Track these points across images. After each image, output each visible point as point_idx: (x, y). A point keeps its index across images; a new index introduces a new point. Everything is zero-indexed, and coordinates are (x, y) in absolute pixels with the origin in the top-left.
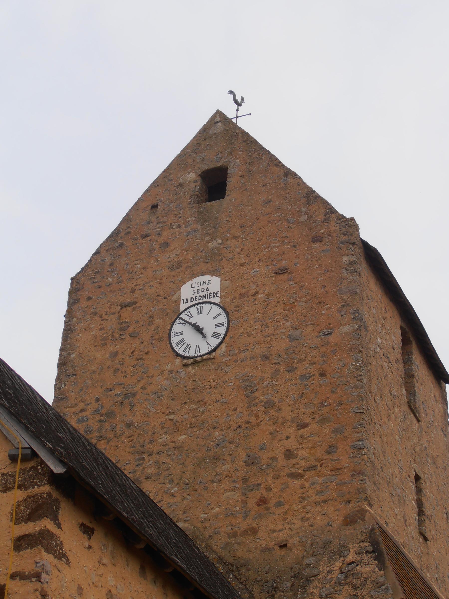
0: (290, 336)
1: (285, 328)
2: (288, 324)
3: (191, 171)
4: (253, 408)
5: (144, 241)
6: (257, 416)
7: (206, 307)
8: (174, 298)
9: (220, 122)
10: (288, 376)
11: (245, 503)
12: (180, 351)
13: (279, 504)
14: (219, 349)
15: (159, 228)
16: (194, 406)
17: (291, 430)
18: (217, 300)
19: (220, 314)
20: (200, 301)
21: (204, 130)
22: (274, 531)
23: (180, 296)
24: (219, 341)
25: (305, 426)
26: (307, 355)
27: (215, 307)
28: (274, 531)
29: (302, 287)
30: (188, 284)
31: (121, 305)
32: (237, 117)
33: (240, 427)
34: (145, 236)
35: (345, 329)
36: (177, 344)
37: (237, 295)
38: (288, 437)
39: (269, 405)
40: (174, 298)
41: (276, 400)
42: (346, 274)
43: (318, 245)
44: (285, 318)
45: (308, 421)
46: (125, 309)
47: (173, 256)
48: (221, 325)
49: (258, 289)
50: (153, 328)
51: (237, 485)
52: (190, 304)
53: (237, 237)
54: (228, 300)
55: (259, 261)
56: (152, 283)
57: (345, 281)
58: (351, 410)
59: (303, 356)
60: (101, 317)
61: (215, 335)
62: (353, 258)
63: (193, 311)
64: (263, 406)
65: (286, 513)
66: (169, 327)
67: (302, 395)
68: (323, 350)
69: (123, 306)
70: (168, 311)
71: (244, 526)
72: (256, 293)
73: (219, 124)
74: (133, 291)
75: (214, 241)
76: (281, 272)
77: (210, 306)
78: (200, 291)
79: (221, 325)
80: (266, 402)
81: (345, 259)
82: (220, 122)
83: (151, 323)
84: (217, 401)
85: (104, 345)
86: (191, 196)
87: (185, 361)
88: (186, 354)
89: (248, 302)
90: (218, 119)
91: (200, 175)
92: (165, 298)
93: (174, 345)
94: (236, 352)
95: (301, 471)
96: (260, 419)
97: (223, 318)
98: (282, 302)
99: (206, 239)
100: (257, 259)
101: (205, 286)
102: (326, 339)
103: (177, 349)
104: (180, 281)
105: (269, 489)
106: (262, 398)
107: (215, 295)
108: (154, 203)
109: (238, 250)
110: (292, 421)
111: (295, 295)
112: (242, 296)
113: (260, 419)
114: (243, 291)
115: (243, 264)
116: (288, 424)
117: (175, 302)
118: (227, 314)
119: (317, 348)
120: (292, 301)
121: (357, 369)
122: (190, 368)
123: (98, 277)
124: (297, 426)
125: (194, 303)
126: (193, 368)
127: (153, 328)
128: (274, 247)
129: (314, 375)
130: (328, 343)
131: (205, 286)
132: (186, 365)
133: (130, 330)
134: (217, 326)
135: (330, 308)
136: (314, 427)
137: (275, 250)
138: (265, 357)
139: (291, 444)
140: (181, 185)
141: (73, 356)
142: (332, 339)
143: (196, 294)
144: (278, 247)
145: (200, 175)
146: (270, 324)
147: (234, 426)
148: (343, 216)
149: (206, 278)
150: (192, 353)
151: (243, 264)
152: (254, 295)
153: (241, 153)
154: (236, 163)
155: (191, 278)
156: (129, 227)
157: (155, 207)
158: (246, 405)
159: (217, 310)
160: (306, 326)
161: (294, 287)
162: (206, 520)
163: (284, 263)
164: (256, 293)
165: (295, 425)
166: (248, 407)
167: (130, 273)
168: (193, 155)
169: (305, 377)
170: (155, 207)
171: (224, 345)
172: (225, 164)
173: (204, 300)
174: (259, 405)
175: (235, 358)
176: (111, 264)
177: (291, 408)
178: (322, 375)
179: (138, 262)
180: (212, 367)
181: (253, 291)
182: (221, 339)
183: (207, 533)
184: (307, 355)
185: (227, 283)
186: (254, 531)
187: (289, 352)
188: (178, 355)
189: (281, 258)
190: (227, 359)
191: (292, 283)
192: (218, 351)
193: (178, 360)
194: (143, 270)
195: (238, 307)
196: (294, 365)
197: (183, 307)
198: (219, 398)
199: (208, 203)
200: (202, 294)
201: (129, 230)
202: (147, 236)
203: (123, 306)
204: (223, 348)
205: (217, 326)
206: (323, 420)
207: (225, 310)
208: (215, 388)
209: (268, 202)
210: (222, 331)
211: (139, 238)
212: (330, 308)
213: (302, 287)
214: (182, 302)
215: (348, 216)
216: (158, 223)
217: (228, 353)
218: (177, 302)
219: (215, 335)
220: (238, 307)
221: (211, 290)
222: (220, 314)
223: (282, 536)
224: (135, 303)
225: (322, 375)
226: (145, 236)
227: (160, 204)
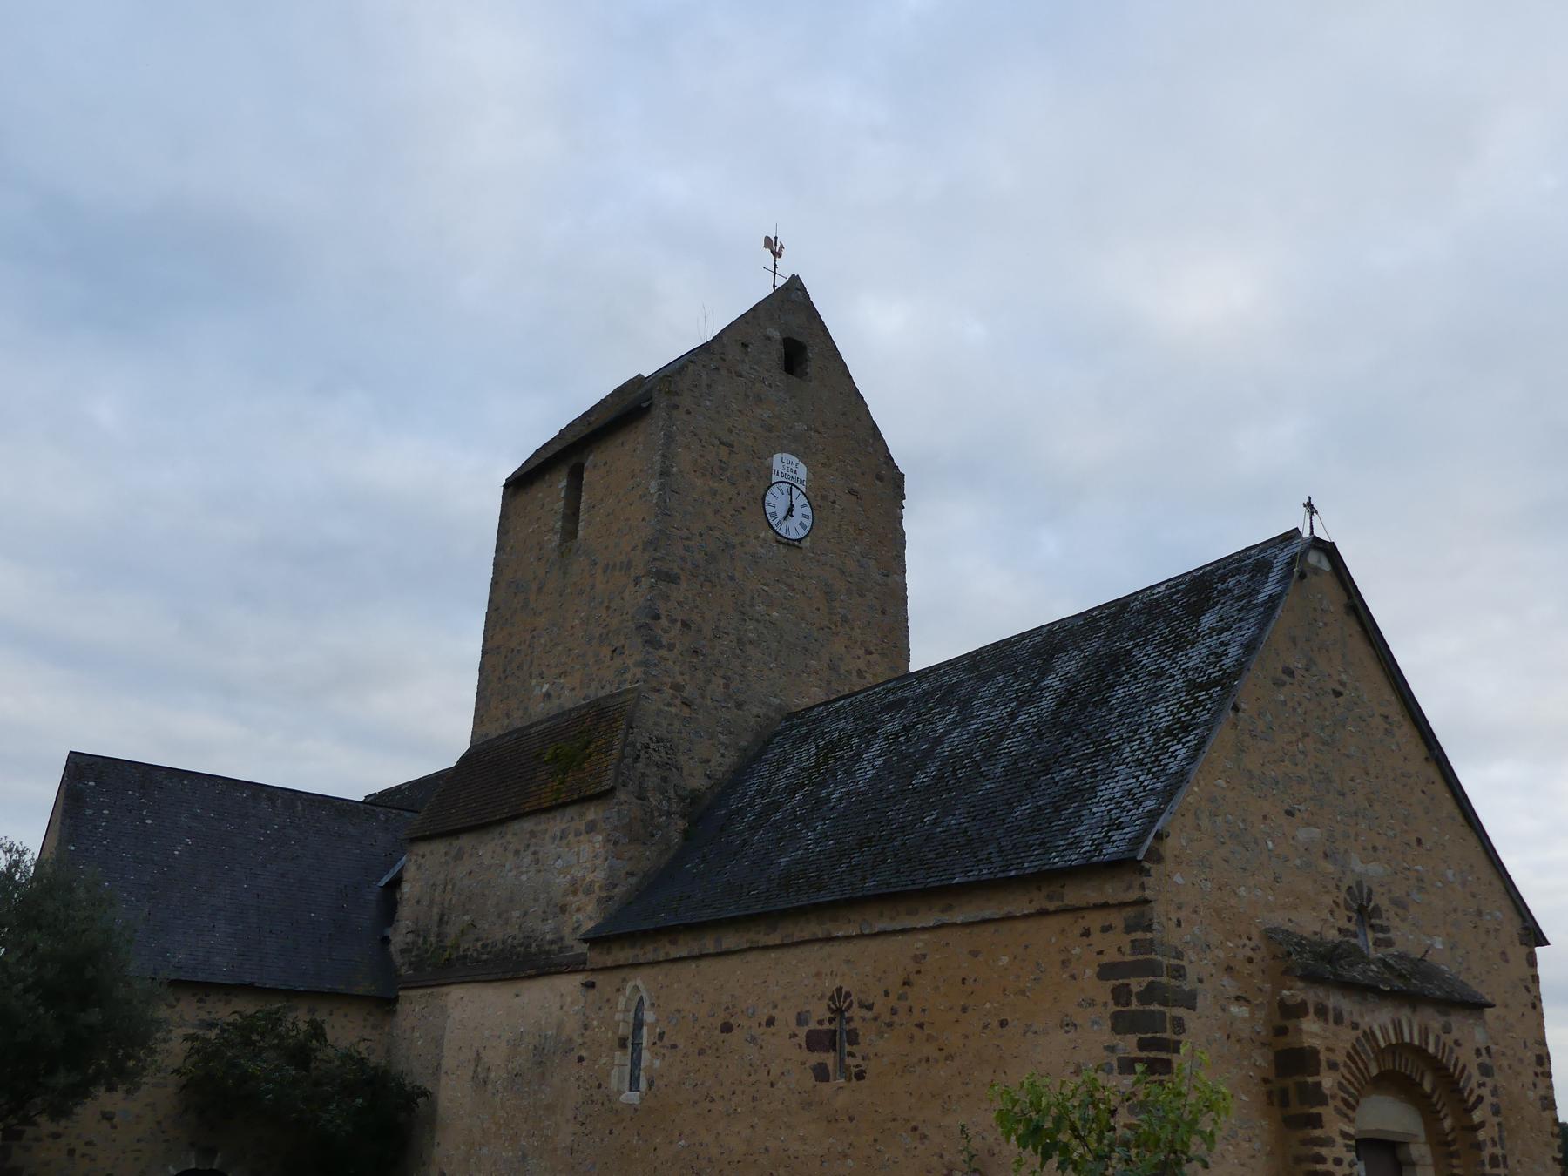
12: (774, 524)
25: (871, 653)
37: (819, 495)
46: (721, 446)
66: (763, 492)
72: (834, 502)
76: (852, 492)
96: (838, 630)
122: (781, 546)
125: (783, 479)
132: (778, 542)
141: (675, 469)
149: (795, 460)
164: (834, 502)
197: (775, 478)
210: (808, 523)
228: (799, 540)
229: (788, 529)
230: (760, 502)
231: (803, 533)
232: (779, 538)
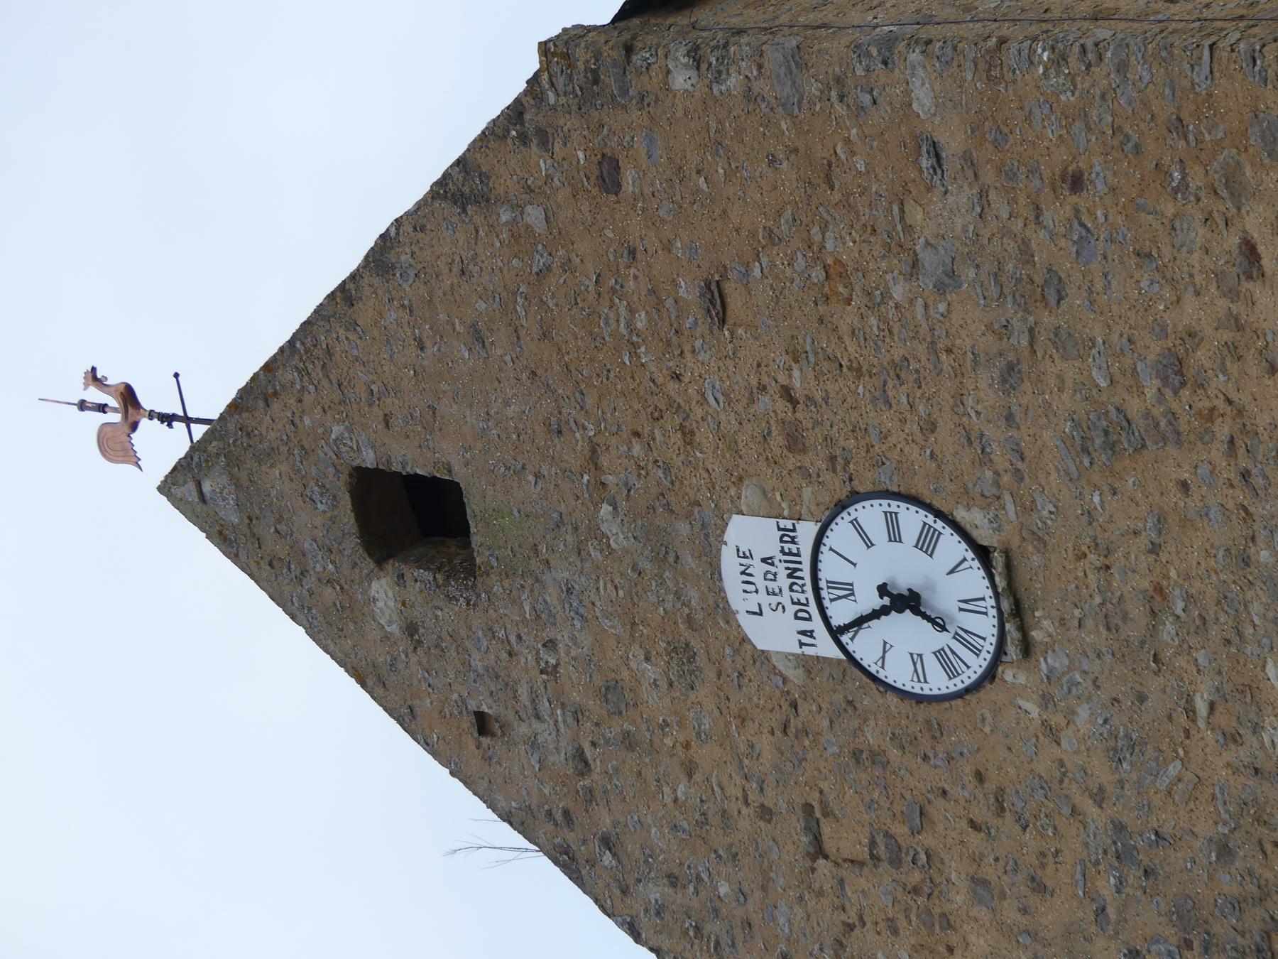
0: (941, 288)
1: (911, 302)
2: (898, 292)
3: (365, 592)
4: (1183, 427)
5: (597, 767)
6: (1210, 415)
7: (831, 568)
8: (796, 675)
9: (199, 485)
10: (1075, 298)
12: (977, 665)
14: (975, 534)
15: (553, 714)
16: (1168, 630)
18: (807, 531)
19: (855, 523)
20: (809, 588)
21: (223, 538)
23: (787, 656)
26: (1005, 232)
27: (832, 539)
29: (773, 238)
30: (750, 626)
31: (814, 858)
32: (188, 420)
33: (1245, 475)
34: (582, 764)
35: (923, 97)
36: (952, 673)
37: (792, 461)
40: (796, 675)
41: (1156, 348)
42: (733, 81)
43: (629, 178)
44: (877, 300)
46: (829, 845)
47: (651, 671)
48: (892, 521)
49: (773, 388)
50: (894, 753)
52: (817, 624)
53: (593, 451)
54: (807, 493)
55: (677, 377)
56: (743, 748)
57: (757, 87)
58: (1202, 89)
59: (1011, 246)
60: (851, 927)
61: (927, 543)
62: (681, 54)
64: (1176, 393)
66: (891, 698)
67: (1143, 255)
68: (989, 176)
69: (818, 850)
70: (839, 698)
72: (787, 393)
73: (207, 487)
74: (766, 813)
75: (604, 528)
77: (826, 557)
78: (773, 586)
79: (892, 521)
80: (1165, 380)
81: (682, 79)
82: (199, 485)
83: (877, 758)
84: (1154, 549)
85: (947, 922)
86: (450, 599)
87: (1012, 651)
88: (989, 646)
89: (817, 423)
90: (189, 490)
91: (380, 563)
92: (794, 705)
93: (957, 685)
94: (989, 474)
96: (1220, 403)
97: (871, 514)
98: (822, 308)
99: (596, 555)
100: (672, 386)
101: (758, 569)
102: (952, 164)
103: (969, 677)
104: (736, 652)
106: (1150, 393)
107: (788, 536)
108: (468, 722)
109: (637, 450)
110: (1233, 294)
111: (800, 263)
112: (795, 442)
113: (1220, 403)
114: (778, 440)
115: (688, 435)
117: (808, 672)
118: (856, 497)
119: (983, 194)
120: (817, 274)
121: (1060, 59)
122: (1036, 634)
123: (714, 928)
124: (1250, 277)
125: (813, 609)
126: (1038, 625)
127: (894, 753)
128: (629, 325)
129: (1077, 211)
130: (967, 158)
131: (758, 569)
132: (1027, 648)
133: (900, 830)
134: (894, 535)
135: (847, 141)
136: (1254, 222)
137: (641, 321)
138: (1010, 375)
140: (411, 629)
142: (953, 142)
143: (785, 600)
144: (632, 311)
145: (380, 563)
146: (897, 354)
147: (1241, 496)
148: (534, 81)
149: (730, 565)
150: (986, 626)
151: (688, 435)
152: (794, 402)
153: (307, 421)
154: (340, 439)
155: (729, 615)
156: (549, 814)
157: (483, 723)
158: (1171, 449)
159: (841, 533)
160: (909, 229)
161: (773, 265)
163: (688, 291)
164: (787, 393)
165: (1246, 285)
166: (1179, 443)
167: (704, 821)
168: (310, 582)
170: (483, 723)
171: (961, 515)
172: (344, 477)
173: (806, 573)
174: (1175, 406)
175: (1006, 479)
176: (673, 880)
177: (1189, 297)
178: (1077, 182)
179: (667, 790)
180: (1036, 560)
181: (782, 405)
182: (939, 525)
184: (1005, 232)
185: (749, 494)
187: (993, 291)
188: (990, 674)
189: (669, 303)
190: (1010, 507)
191: (757, 272)
192: (984, 536)
193: (1007, 674)
194: (698, 777)
195: (833, 459)
196: (1039, 279)
197: (826, 648)
198: (1142, 542)
199: (476, 540)
200: (783, 581)
201: (559, 816)
202: (580, 755)
203: (818, 850)
204: (971, 517)
205: (894, 535)
206: (1234, 186)
207: (841, 506)
208: (1108, 552)
209: (477, 337)
210: (912, 519)
211: (587, 782)
212: (847, 141)
213: (773, 238)
214: (809, 651)
215: (532, 64)
216: (538, 717)
217: (991, 501)
218: (810, 665)
219: (927, 543)
220: (833, 459)
221: (773, 549)
222: (855, 523)
224: (808, 808)
225: (1077, 182)
226: (582, 764)
227: (473, 706)
228: (983, 554)
229: (968, 605)
230: (934, 711)
231: (951, 547)
232: (1012, 651)
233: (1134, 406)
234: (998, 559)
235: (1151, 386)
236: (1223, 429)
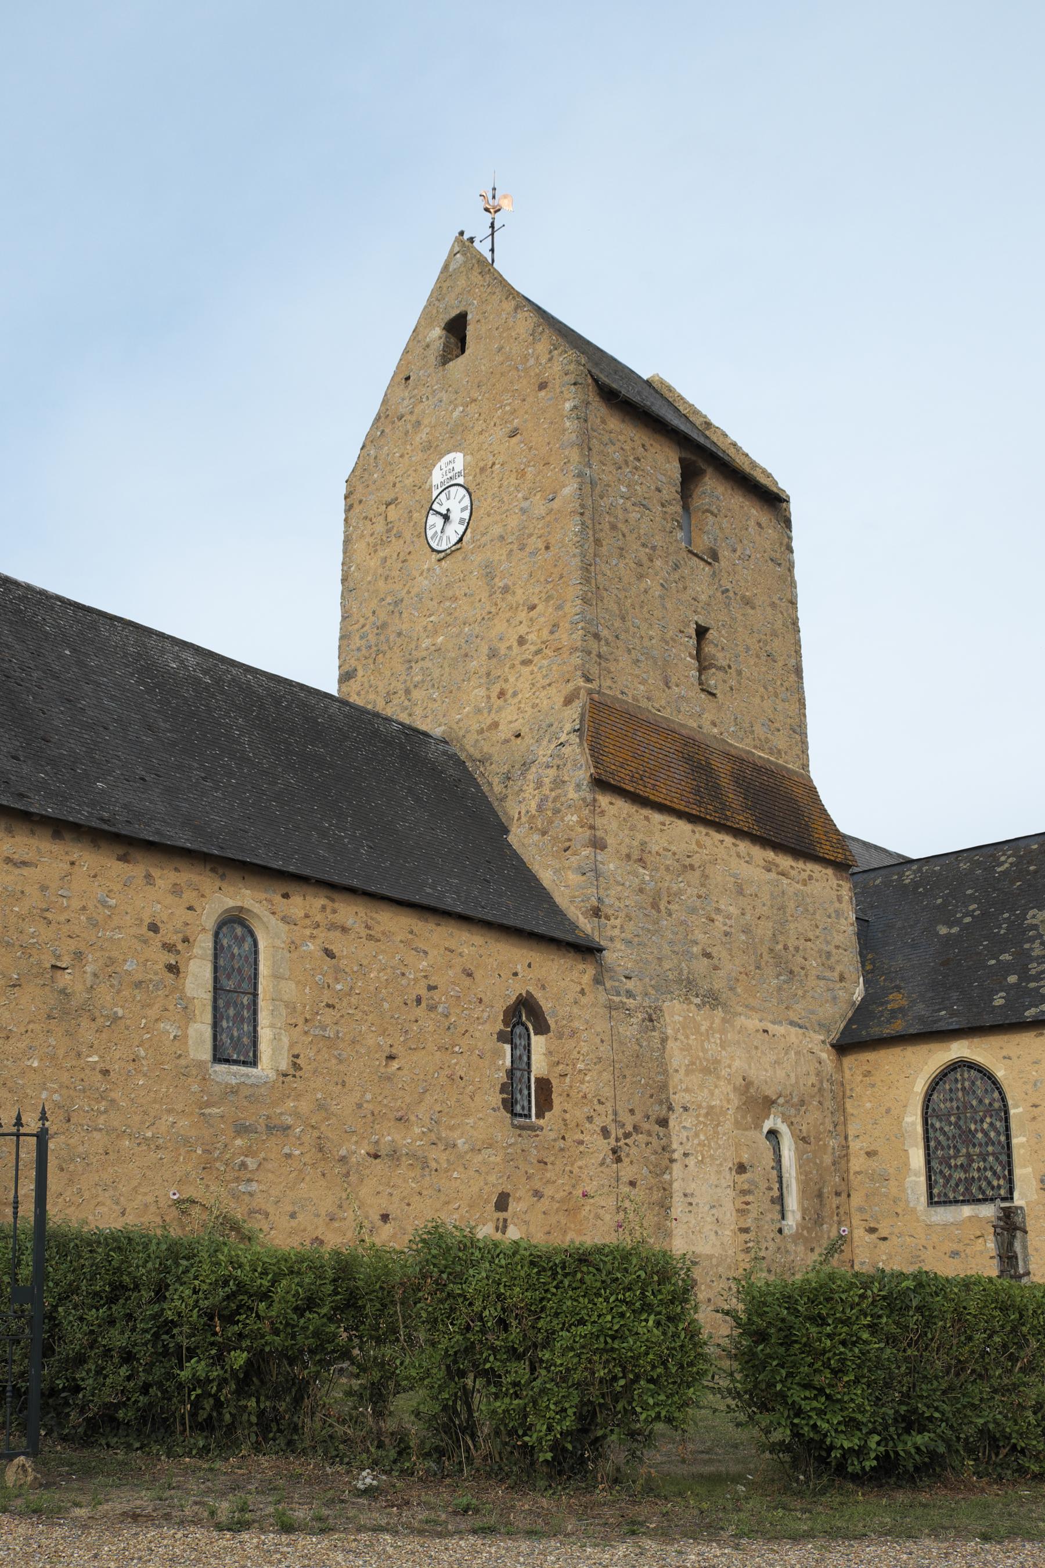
7: (453, 489)
11: (489, 697)
13: (515, 694)
16: (448, 604)
17: (523, 615)
18: (461, 480)
22: (511, 722)
24: (464, 527)
28: (511, 722)
30: (438, 467)
38: (521, 623)
39: (506, 590)
45: (536, 601)
51: (482, 681)
52: (440, 489)
63: (443, 496)
65: (520, 702)
71: (489, 721)
95: (530, 657)
101: (450, 466)
105: (506, 681)
107: (459, 474)
108: (407, 374)
110: (523, 605)
116: (521, 608)
131: (450, 466)
136: (540, 608)
138: (502, 538)
139: (522, 630)
147: (479, 619)
155: (440, 459)
157: (408, 378)
159: (462, 492)
162: (460, 720)
169: (533, 554)
170: (408, 378)
171: (469, 530)
183: (461, 733)
186: (495, 725)
197: (435, 494)
200: (449, 475)
207: (467, 490)
223: (516, 726)
228: (461, 540)
233: (497, 580)
234: (458, 546)
235: (501, 584)
236: (493, 610)
